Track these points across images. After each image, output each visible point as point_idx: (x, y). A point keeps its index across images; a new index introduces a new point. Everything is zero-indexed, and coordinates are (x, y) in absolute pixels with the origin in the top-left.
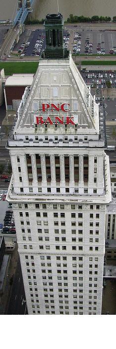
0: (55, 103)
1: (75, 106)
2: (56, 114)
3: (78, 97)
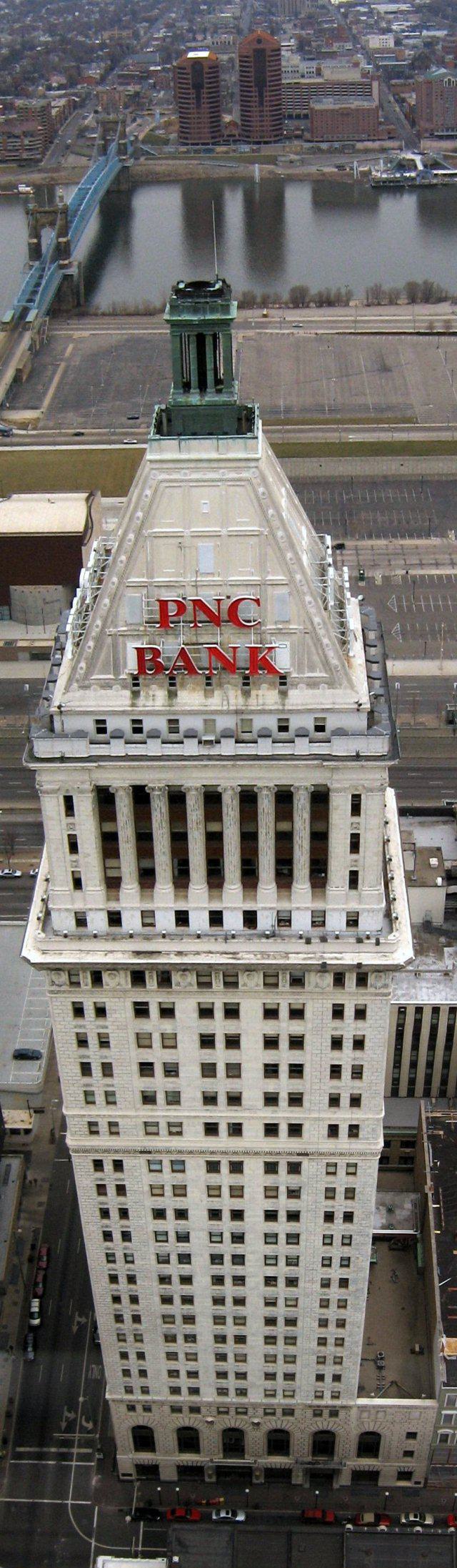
0: (208, 596)
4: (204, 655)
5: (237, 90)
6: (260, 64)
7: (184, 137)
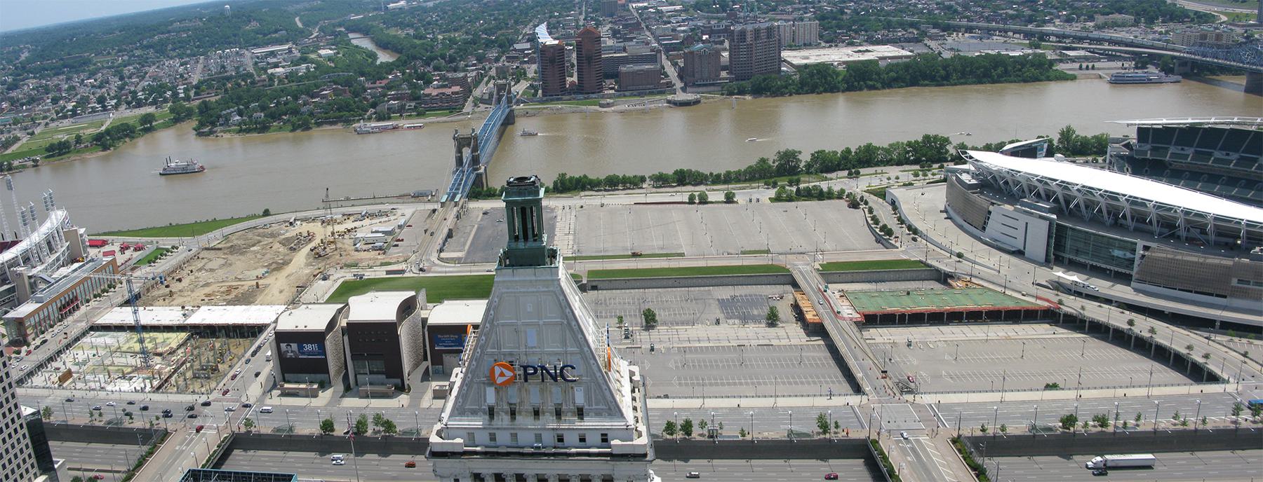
6: (588, 45)
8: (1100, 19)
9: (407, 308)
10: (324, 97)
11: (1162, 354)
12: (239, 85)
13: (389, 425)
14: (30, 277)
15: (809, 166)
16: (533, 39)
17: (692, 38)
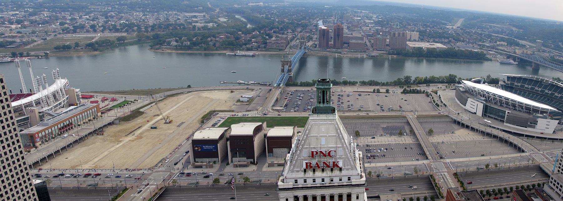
0: (323, 150)
1: (340, 152)
2: (324, 159)
3: (343, 145)
4: (322, 164)
5: (333, 37)
6: (338, 32)
7: (320, 46)
8: (498, 43)
9: (258, 130)
10: (221, 38)
11: (511, 144)
12: (176, 28)
13: (246, 179)
14: (40, 113)
15: (414, 81)
16: (316, 26)
17: (377, 32)
